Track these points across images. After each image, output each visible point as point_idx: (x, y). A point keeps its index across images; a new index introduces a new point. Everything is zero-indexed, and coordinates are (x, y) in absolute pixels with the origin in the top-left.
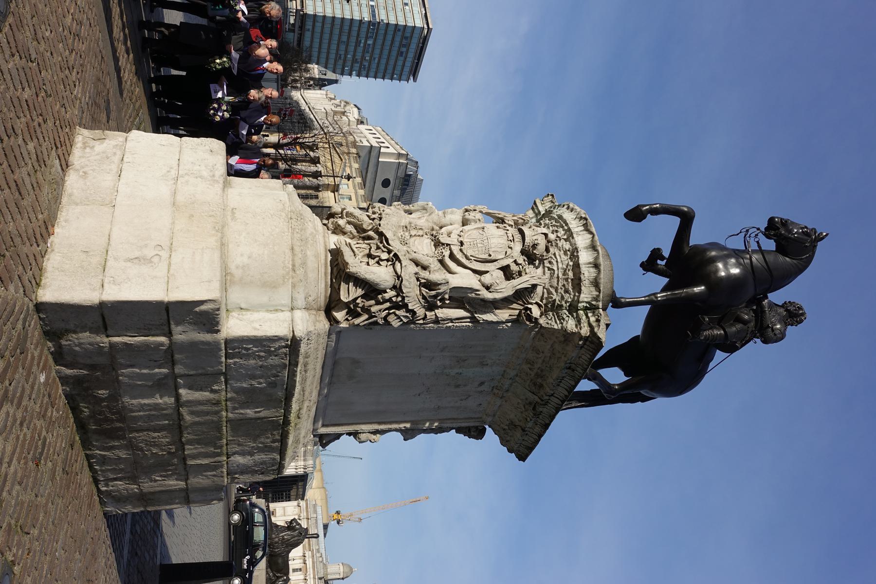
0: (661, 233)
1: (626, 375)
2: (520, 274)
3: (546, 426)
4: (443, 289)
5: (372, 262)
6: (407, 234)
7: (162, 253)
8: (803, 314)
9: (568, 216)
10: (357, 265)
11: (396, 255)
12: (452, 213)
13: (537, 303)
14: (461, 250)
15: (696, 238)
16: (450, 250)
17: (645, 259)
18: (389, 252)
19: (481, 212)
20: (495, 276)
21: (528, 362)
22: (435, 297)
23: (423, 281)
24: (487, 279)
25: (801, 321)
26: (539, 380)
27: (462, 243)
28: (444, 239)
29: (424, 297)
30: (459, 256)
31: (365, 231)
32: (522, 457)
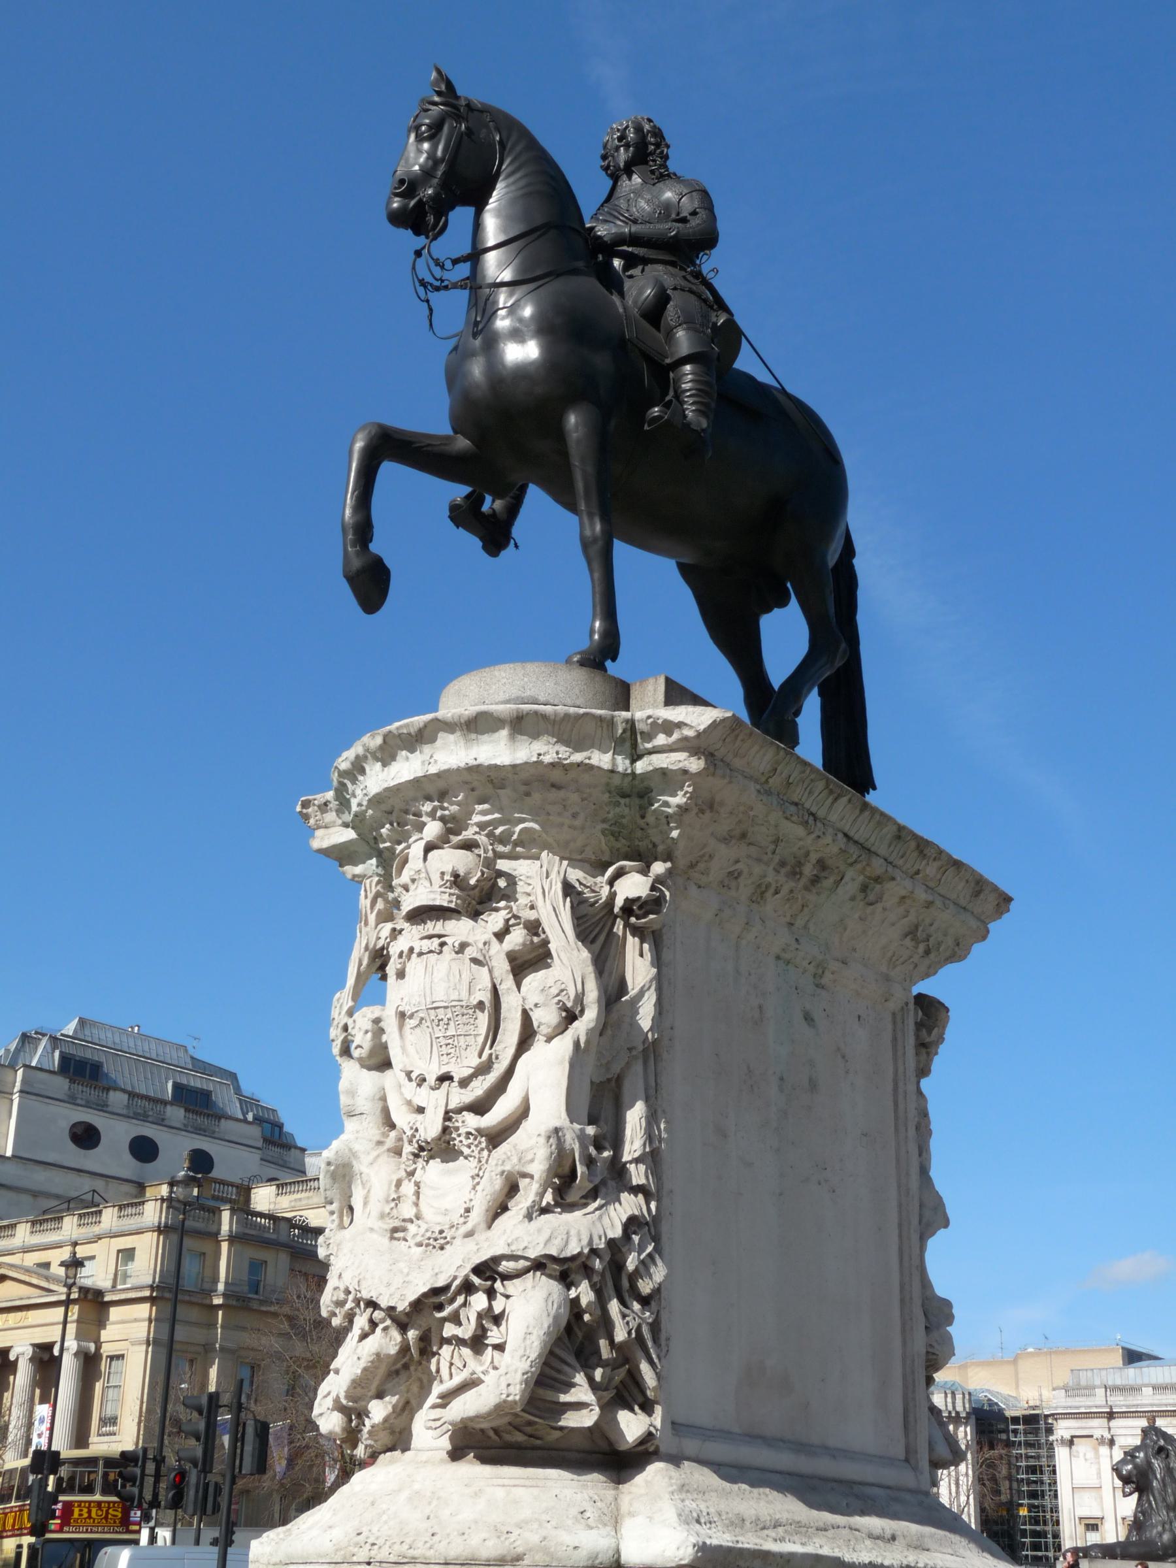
0: (416, 505)
1: (783, 602)
2: (534, 927)
3: (923, 846)
4: (572, 1143)
5: (494, 1335)
6: (412, 1228)
8: (639, 129)
9: (377, 779)
10: (499, 1378)
11: (478, 1270)
12: (352, 1093)
13: (611, 883)
14: (464, 1083)
15: (432, 417)
16: (459, 1111)
17: (475, 543)
18: (468, 1288)
19: (350, 1013)
20: (539, 993)
21: (760, 893)
22: (590, 1162)
23: (549, 1198)
24: (544, 1018)
25: (658, 133)
26: (808, 870)
27: (445, 1078)
28: (430, 1128)
29: (593, 1194)
30: (479, 1088)
31: (405, 1349)
32: (1004, 901)
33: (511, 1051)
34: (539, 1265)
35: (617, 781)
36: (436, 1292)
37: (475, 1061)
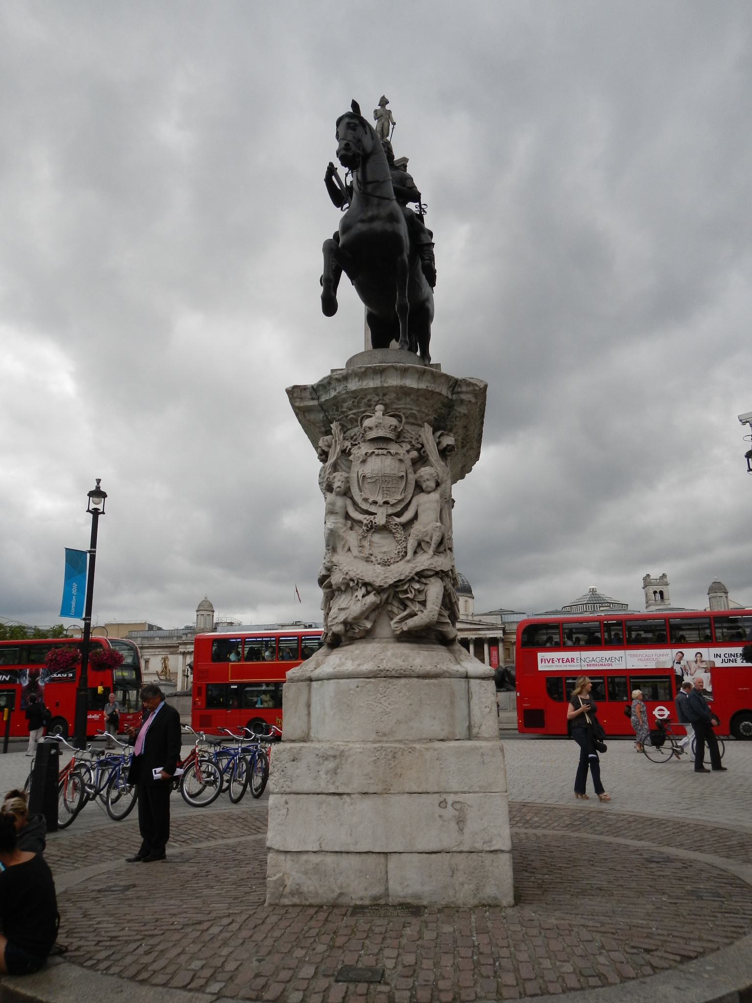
2: (421, 448)
7: (450, 803)
11: (417, 574)
14: (393, 505)
27: (386, 503)
30: (399, 508)
33: (411, 496)
34: (437, 574)
35: (445, 401)
36: (400, 581)
37: (399, 498)
